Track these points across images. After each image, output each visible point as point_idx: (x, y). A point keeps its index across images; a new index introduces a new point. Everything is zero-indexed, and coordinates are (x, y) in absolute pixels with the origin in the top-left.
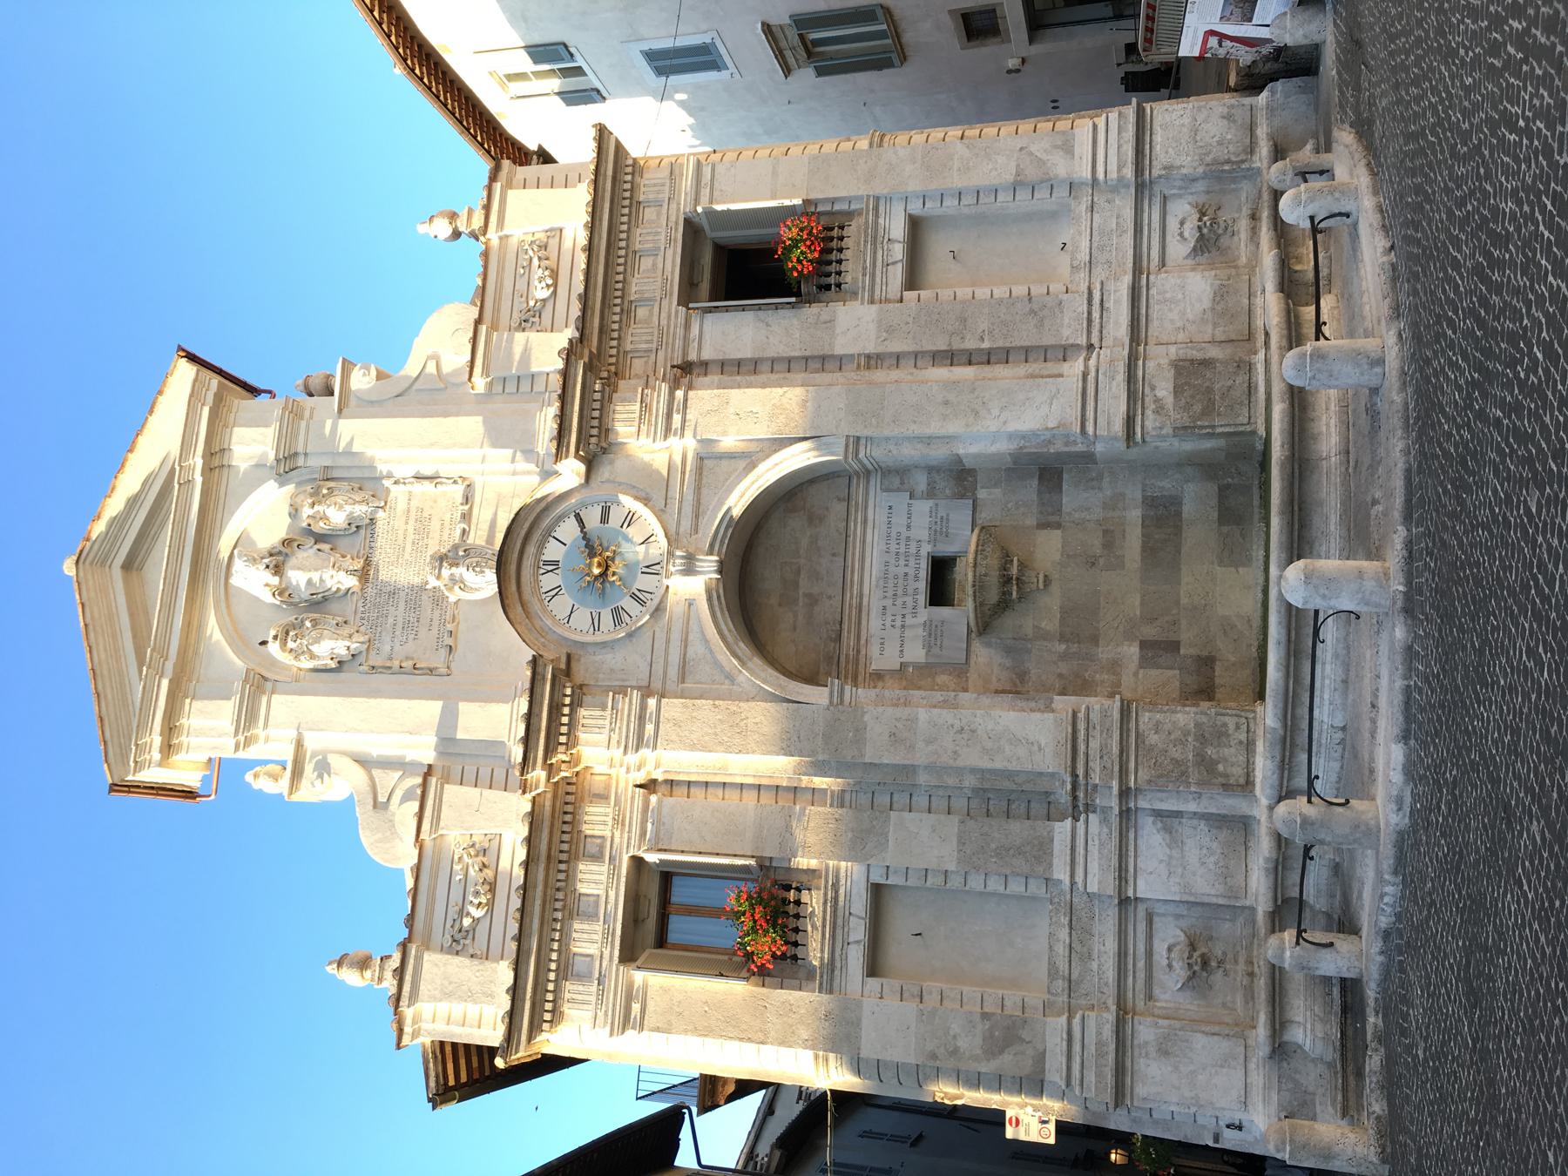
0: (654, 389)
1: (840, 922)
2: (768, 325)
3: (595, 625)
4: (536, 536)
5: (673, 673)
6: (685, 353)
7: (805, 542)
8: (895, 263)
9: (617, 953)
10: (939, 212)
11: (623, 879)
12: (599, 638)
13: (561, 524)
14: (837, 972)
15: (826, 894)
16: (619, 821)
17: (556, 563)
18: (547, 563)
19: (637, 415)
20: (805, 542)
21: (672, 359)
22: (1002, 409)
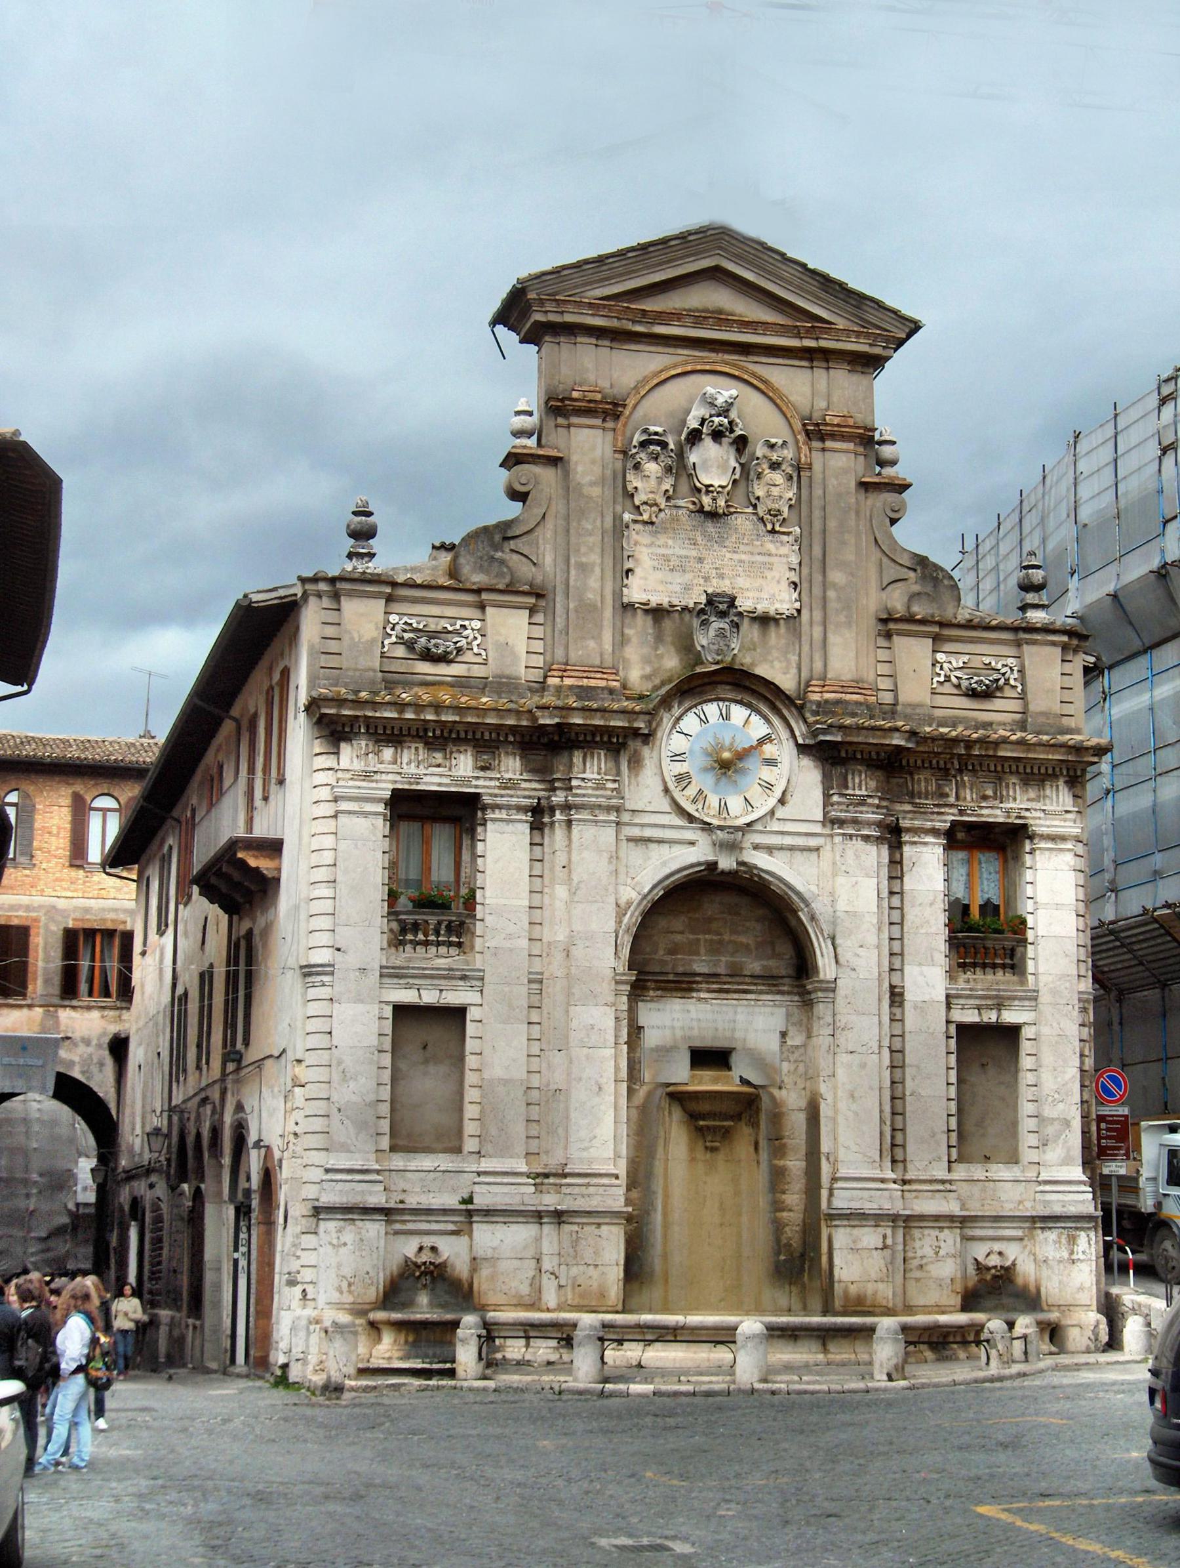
0: (878, 807)
1: (436, 982)
2: (931, 904)
3: (677, 757)
4: (748, 698)
5: (636, 832)
6: (908, 830)
7: (743, 939)
8: (980, 1014)
9: (400, 786)
10: (1022, 1053)
11: (461, 790)
12: (666, 762)
13: (762, 721)
14: (395, 981)
15: (458, 970)
16: (508, 785)
17: (728, 718)
18: (728, 708)
19: (858, 792)
20: (743, 939)
21: (904, 818)
22: (856, 1114)
